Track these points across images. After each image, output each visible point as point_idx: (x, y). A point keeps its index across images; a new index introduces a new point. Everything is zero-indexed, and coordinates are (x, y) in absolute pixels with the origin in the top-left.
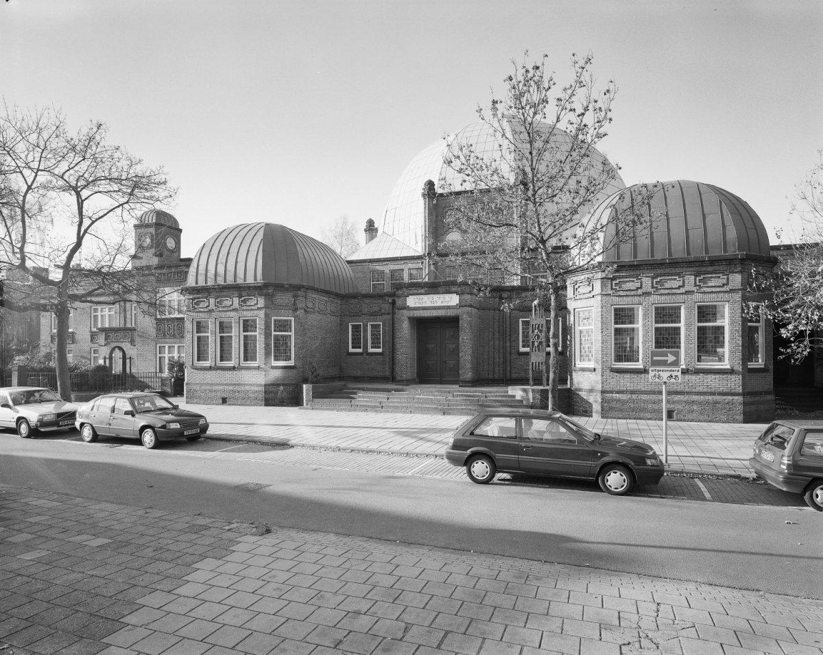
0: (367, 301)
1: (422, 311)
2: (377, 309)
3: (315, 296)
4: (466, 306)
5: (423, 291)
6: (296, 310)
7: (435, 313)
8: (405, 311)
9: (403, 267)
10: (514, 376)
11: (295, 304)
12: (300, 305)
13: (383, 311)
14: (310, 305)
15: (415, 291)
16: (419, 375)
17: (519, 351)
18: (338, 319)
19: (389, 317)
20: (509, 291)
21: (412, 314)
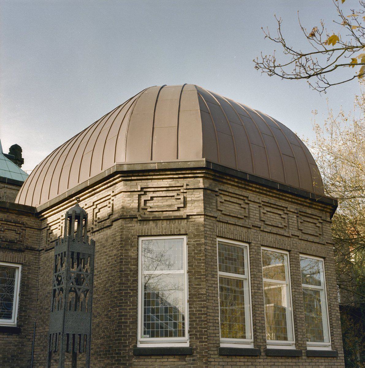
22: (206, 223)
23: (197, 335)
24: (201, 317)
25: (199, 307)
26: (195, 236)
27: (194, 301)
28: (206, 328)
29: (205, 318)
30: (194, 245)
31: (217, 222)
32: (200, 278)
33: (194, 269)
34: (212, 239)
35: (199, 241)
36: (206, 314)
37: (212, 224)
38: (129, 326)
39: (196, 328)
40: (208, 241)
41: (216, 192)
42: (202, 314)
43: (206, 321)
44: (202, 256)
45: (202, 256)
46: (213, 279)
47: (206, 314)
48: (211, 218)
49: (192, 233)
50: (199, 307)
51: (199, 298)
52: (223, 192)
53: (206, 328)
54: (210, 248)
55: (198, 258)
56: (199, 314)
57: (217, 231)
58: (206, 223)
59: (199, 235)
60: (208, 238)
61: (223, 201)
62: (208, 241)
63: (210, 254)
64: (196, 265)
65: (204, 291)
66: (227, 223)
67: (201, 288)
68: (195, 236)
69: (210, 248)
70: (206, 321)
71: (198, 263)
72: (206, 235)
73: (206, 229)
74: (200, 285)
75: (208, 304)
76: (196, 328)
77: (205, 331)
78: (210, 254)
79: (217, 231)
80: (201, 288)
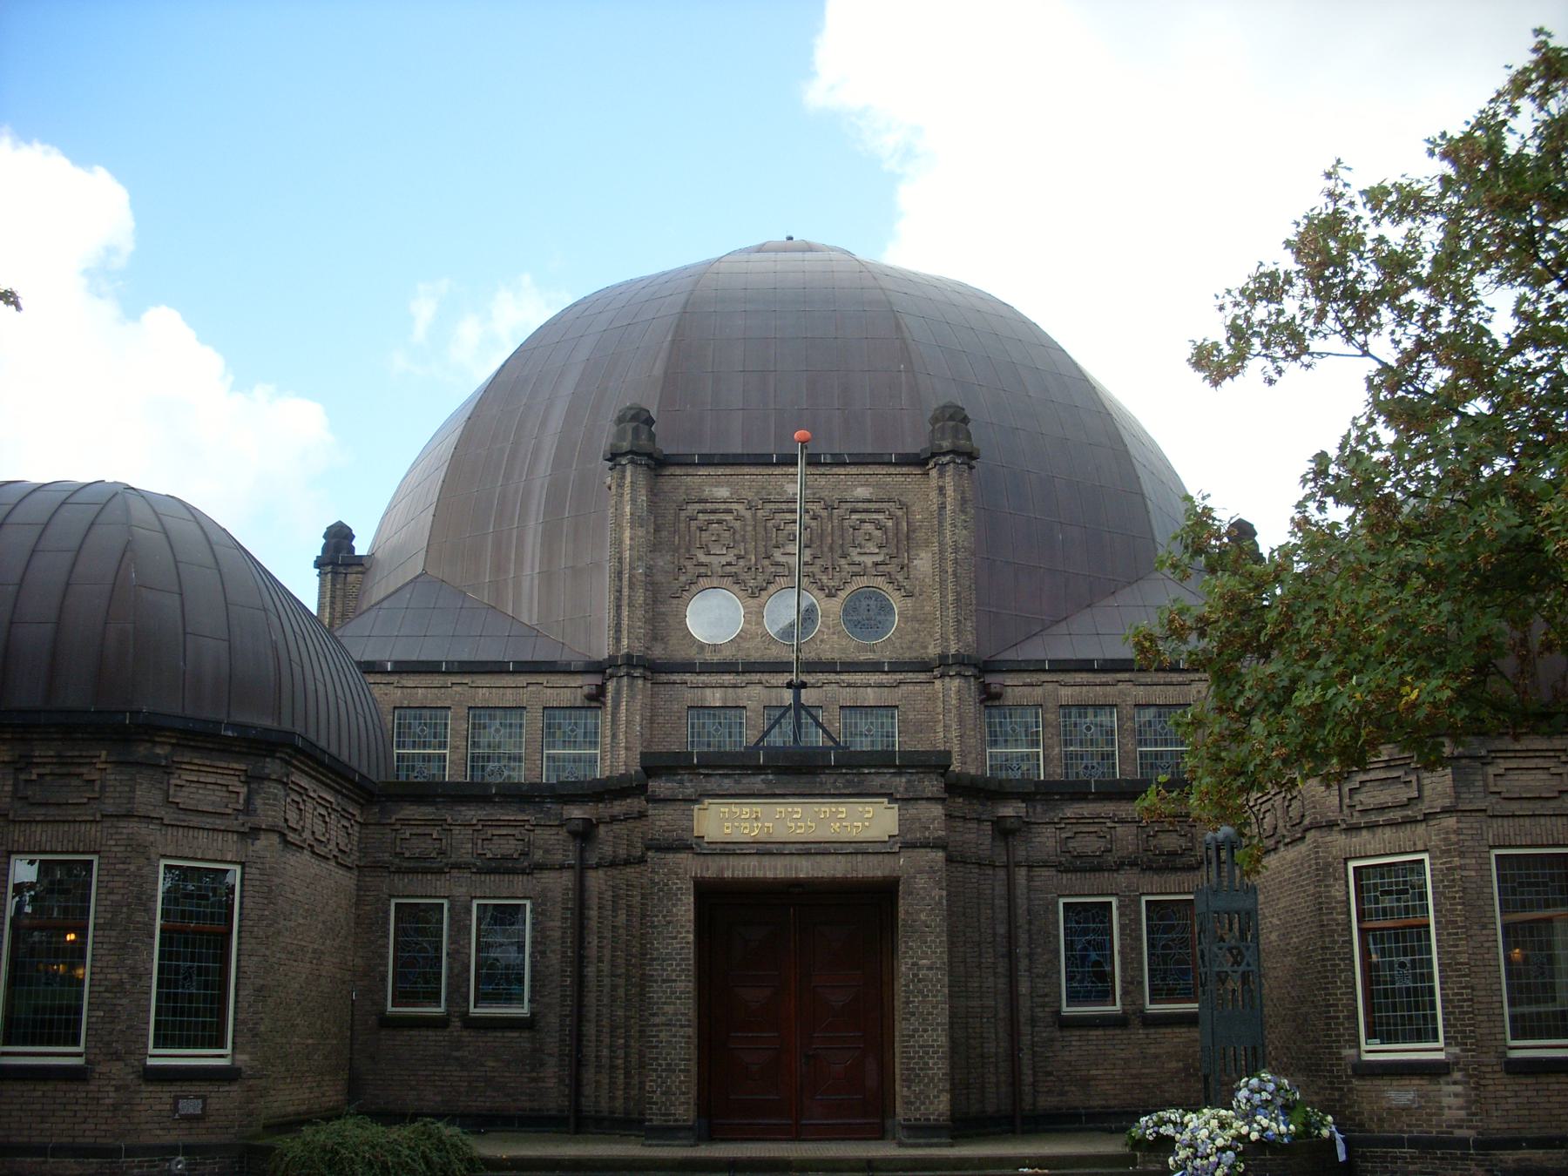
0: (472, 814)
1: (753, 862)
2: (510, 847)
3: (305, 782)
4: (925, 845)
5: (757, 782)
6: (255, 832)
7: (805, 869)
8: (684, 858)
9: (524, 697)
10: (1047, 1102)
11: (248, 809)
12: (266, 815)
13: (538, 856)
14: (292, 816)
15: (727, 783)
16: (705, 1106)
17: (1058, 1012)
18: (348, 880)
19: (567, 879)
20: (1025, 797)
21: (712, 869)
22: (1460, 825)
23: (1457, 1037)
24: (1462, 1007)
25: (1459, 988)
26: (1443, 852)
27: (1449, 977)
28: (1470, 1025)
29: (1469, 1006)
30: (1441, 870)
31: (1489, 820)
32: (1457, 934)
33: (1445, 916)
34: (1477, 855)
35: (1450, 862)
36: (1471, 1000)
37: (1475, 825)
38: (1342, 1024)
39: (1454, 1026)
40: (1468, 861)
41: (1482, 757)
42: (1465, 1001)
43: (1472, 1012)
44: (1457, 892)
45: (1457, 892)
46: (1484, 932)
47: (1471, 1000)
48: (1473, 814)
49: (1437, 846)
50: (1459, 988)
51: (1456, 970)
52: (1498, 755)
53: (1470, 1025)
54: (1473, 873)
55: (1451, 895)
56: (1459, 1000)
57: (1491, 835)
58: (1460, 825)
59: (1449, 851)
60: (1467, 855)
61: (1502, 771)
62: (1468, 861)
63: (1474, 886)
64: (1447, 910)
65: (1463, 958)
66: (1513, 816)
67: (1459, 952)
68: (1443, 852)
69: (1473, 873)
70: (1472, 1012)
71: (1451, 904)
72: (1463, 849)
73: (1461, 837)
74: (1457, 946)
75: (1475, 981)
76: (1454, 1026)
77: (1471, 1031)
78: (1474, 886)
79: (1491, 835)
80: (1459, 952)
